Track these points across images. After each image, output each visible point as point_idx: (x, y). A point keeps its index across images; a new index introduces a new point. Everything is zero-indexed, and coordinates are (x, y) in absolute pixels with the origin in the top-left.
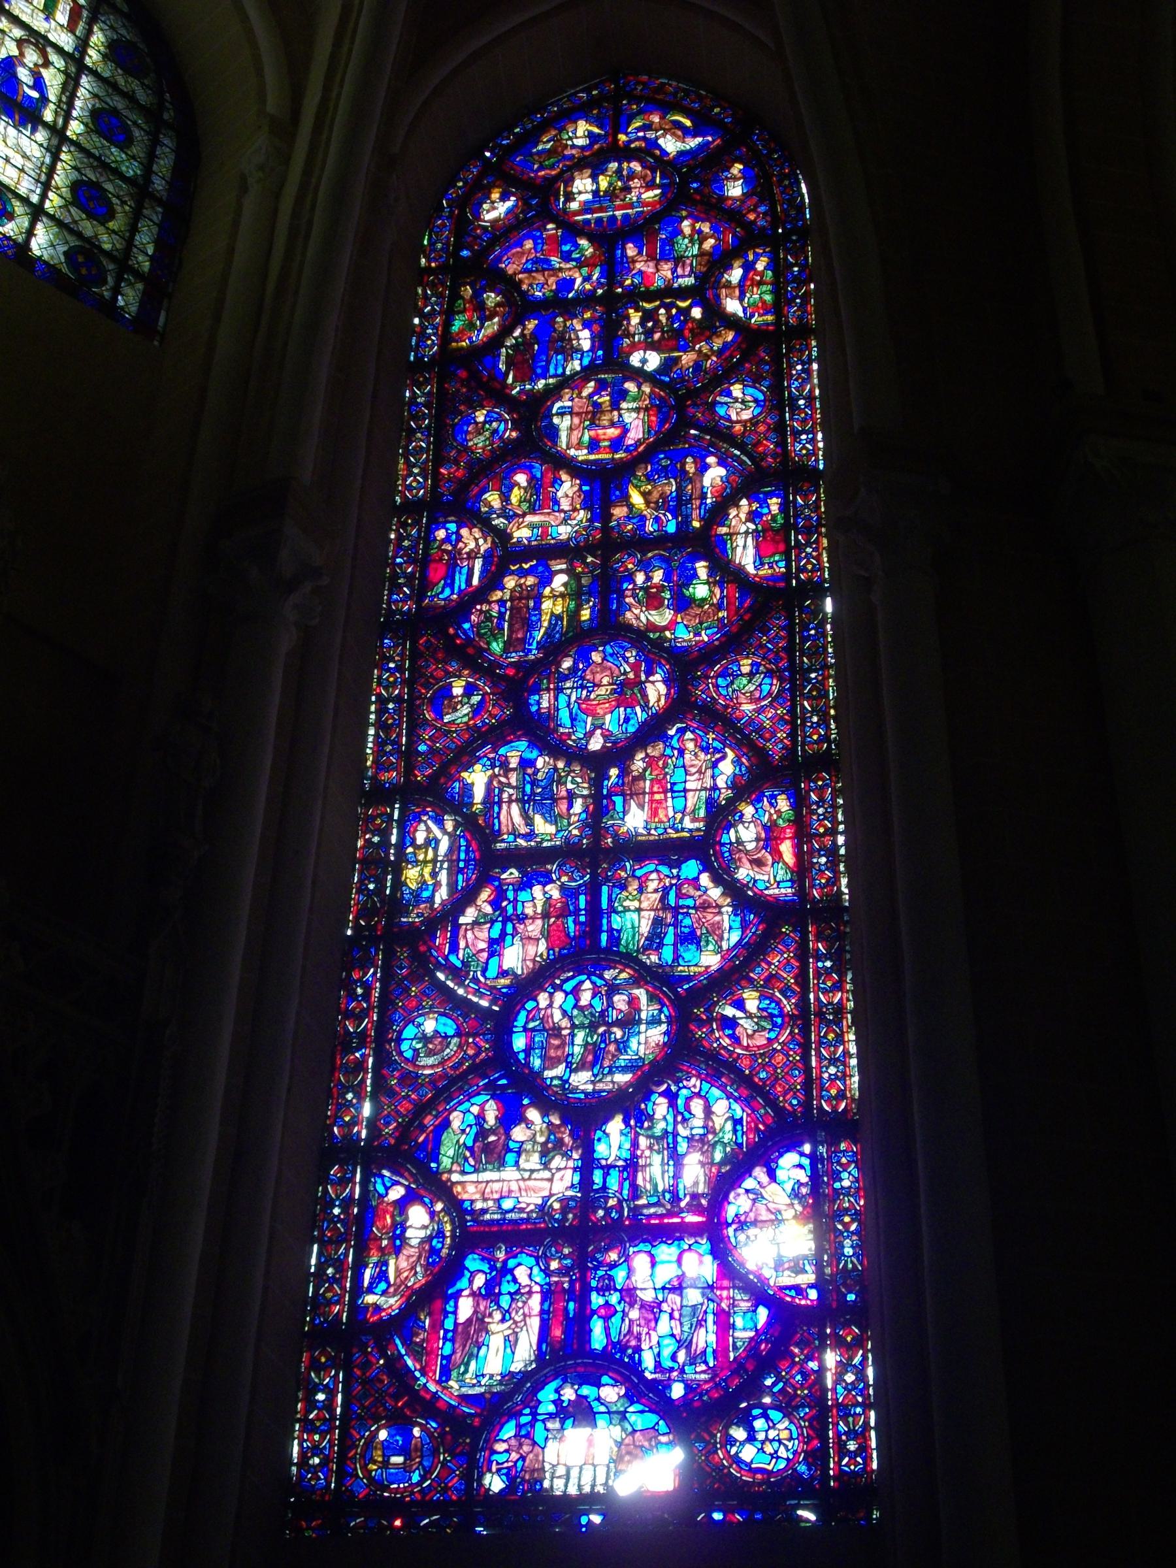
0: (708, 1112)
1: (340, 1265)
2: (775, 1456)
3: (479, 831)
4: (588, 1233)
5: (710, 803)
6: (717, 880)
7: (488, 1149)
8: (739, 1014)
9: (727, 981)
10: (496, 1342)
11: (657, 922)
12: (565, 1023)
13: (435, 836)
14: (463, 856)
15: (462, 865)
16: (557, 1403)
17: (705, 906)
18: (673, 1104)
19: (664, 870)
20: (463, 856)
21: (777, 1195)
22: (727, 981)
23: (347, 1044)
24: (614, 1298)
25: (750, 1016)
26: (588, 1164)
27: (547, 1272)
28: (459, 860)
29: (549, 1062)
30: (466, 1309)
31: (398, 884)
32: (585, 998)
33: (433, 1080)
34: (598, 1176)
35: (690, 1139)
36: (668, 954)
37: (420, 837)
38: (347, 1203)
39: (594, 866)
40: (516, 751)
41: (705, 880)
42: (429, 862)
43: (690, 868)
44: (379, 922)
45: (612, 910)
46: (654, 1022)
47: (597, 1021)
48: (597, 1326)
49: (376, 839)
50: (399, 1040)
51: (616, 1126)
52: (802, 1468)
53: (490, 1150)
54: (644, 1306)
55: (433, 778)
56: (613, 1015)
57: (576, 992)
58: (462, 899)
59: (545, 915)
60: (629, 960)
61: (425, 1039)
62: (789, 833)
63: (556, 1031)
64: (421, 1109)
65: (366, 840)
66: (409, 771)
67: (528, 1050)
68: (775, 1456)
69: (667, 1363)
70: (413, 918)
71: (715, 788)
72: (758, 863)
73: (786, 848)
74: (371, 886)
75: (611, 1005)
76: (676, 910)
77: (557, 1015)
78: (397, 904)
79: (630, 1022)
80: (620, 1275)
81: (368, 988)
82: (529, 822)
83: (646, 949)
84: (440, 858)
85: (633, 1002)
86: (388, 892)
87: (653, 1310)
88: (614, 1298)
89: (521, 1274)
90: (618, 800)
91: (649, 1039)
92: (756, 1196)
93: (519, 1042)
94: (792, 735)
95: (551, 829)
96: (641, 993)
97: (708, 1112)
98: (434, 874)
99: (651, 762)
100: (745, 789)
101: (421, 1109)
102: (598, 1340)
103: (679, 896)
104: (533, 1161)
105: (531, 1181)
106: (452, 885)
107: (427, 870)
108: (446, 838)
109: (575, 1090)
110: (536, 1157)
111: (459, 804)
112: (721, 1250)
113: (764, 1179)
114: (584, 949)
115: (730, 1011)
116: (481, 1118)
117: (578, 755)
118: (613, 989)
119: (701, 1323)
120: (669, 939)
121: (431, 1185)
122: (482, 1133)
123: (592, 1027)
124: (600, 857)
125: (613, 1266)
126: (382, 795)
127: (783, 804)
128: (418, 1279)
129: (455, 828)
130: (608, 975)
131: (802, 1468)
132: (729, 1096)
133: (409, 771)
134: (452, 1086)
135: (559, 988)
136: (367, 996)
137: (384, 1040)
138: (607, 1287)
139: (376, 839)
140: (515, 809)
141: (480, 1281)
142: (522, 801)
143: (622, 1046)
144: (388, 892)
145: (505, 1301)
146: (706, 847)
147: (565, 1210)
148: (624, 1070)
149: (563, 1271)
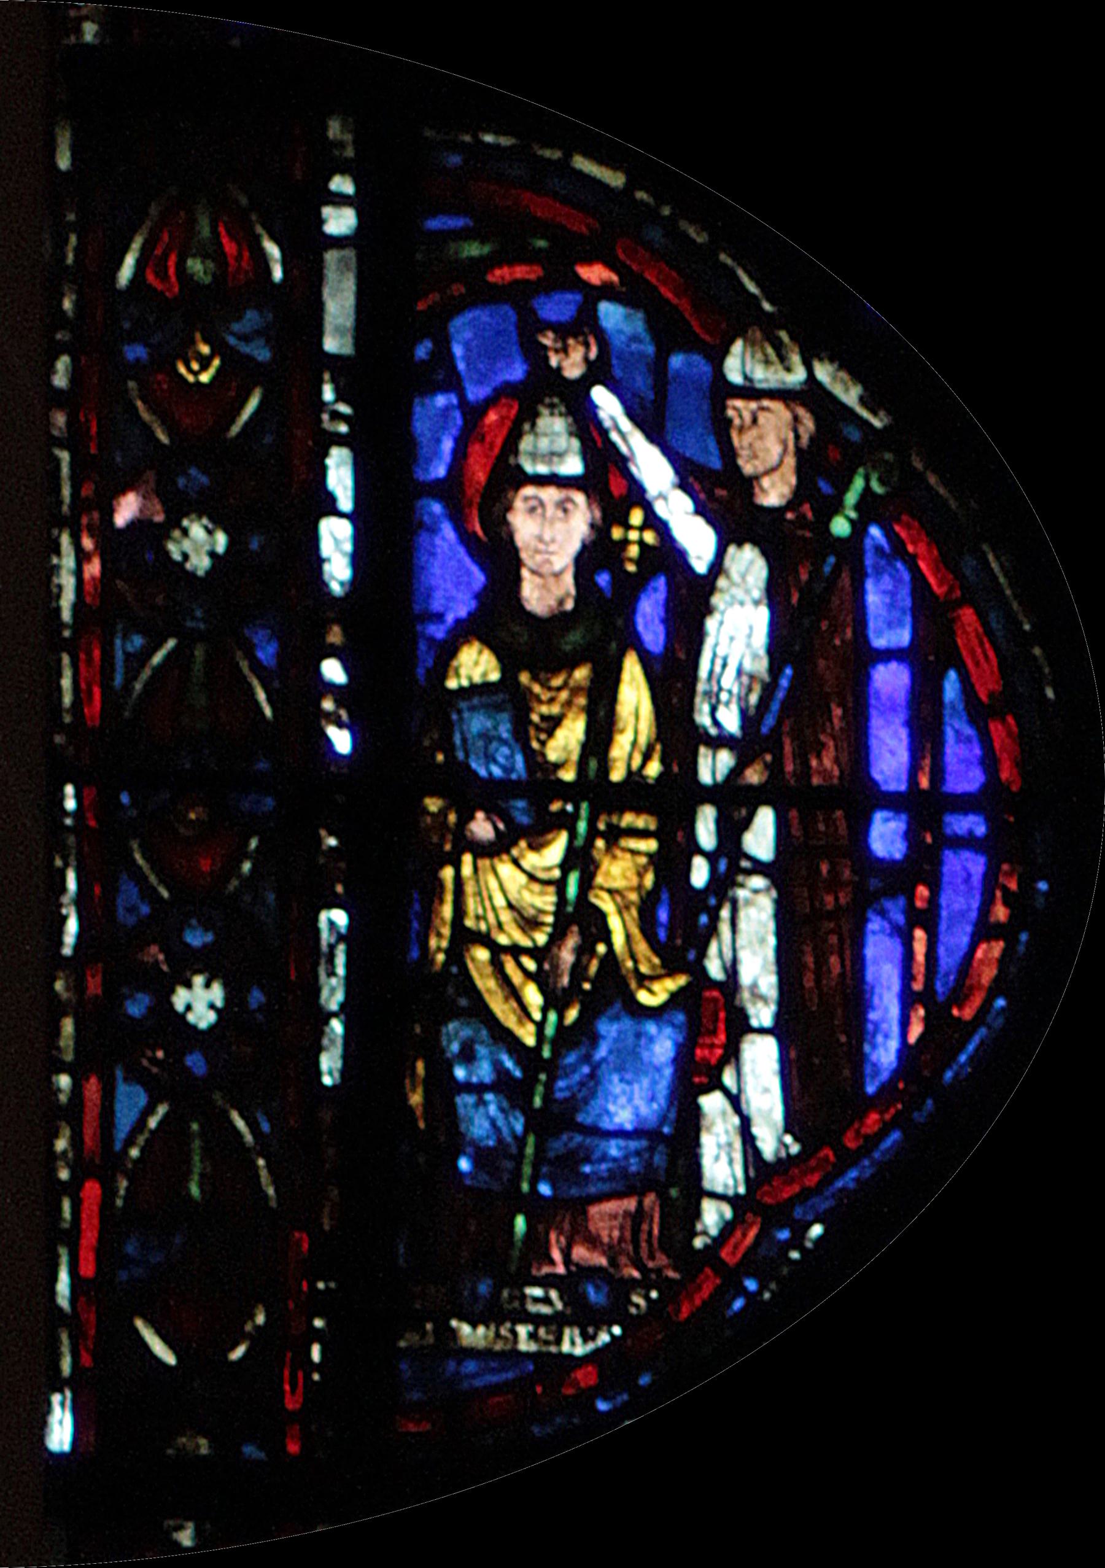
14: (890, 757)
15: (886, 836)
20: (890, 757)
28: (861, 796)
42: (634, 793)
44: (280, 1345)
49: (199, 544)
65: (111, 541)
74: (200, 1002)
84: (713, 766)
86: (330, 1065)
107: (620, 872)
108: (748, 566)
129: (820, 465)
139: (199, 544)
144: (330, 1065)
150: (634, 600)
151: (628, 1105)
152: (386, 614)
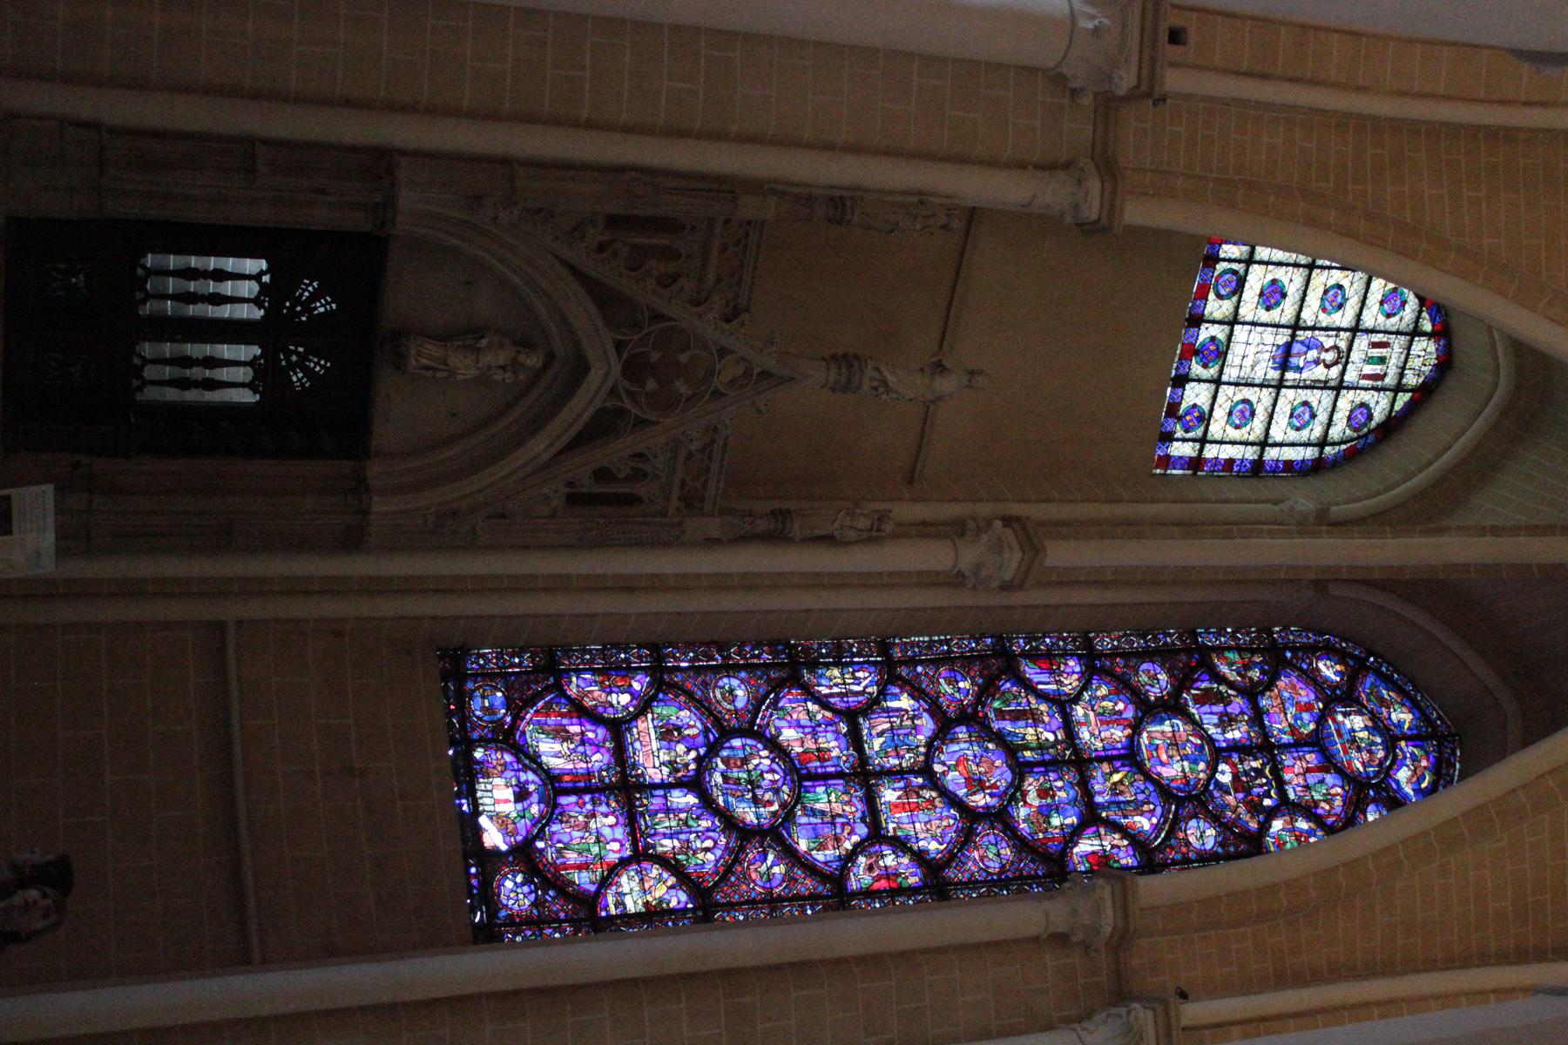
0: (707, 850)
1: (592, 661)
2: (509, 898)
3: (871, 706)
4: (626, 789)
5: (907, 837)
6: (856, 846)
7: (669, 732)
8: (769, 863)
9: (789, 854)
10: (557, 747)
11: (823, 813)
12: (751, 767)
13: (864, 681)
16: (527, 782)
17: (837, 839)
18: (708, 830)
19: (858, 815)
21: (660, 891)
22: (789, 854)
23: (722, 647)
24: (589, 807)
25: (768, 869)
26: (666, 786)
27: (601, 770)
29: (726, 761)
30: (575, 729)
31: (827, 666)
32: (768, 776)
33: (708, 699)
34: (661, 792)
35: (688, 841)
36: (804, 820)
37: (860, 674)
38: (626, 660)
39: (855, 774)
40: (927, 724)
41: (855, 839)
43: (862, 830)
45: (827, 786)
46: (758, 816)
47: (753, 784)
48: (573, 799)
50: (728, 676)
51: (691, 799)
52: (503, 913)
53: (668, 733)
54: (587, 823)
55: (900, 677)
56: (759, 792)
57: (772, 771)
58: (823, 702)
59: (818, 750)
60: (798, 800)
61: (731, 691)
62: (894, 885)
63: (745, 761)
64: (690, 695)
66: (901, 663)
67: (732, 748)
68: (509, 898)
69: (556, 837)
70: (806, 676)
71: (918, 839)
72: (870, 868)
73: (883, 884)
75: (766, 791)
76: (833, 824)
77: (755, 762)
78: (813, 665)
79: (756, 801)
80: (603, 809)
81: (758, 657)
82: (880, 735)
83: (804, 808)
85: (770, 803)
87: (586, 827)
88: (589, 807)
89: (598, 756)
90: (902, 784)
91: (747, 813)
92: (660, 879)
93: (737, 742)
94: (960, 883)
95: (877, 748)
96: (776, 807)
97: (707, 850)
98: (836, 685)
99: (931, 801)
100: (920, 857)
101: (690, 695)
102: (564, 800)
103: (843, 825)
104: (664, 757)
105: (652, 757)
106: (832, 695)
109: (711, 776)
110: (667, 758)
111: (883, 694)
112: (624, 863)
113: (669, 883)
114: (802, 774)
115: (771, 857)
116: (690, 727)
117: (929, 757)
118: (777, 791)
119: (580, 854)
120: (813, 820)
121: (644, 706)
122: (679, 728)
123: (750, 782)
124: (864, 776)
125: (608, 805)
126: (884, 648)
127: (913, 880)
128: (588, 703)
130: (785, 788)
131: (503, 913)
132: (717, 861)
133: (901, 663)
134: (704, 707)
135: (773, 761)
136: (754, 656)
137: (729, 669)
138: (593, 801)
140: (887, 726)
141: (591, 735)
142: (892, 728)
143: (741, 798)
145: (581, 749)
146: (877, 836)
147: (637, 776)
148: (726, 802)
149: (601, 779)
150: (858, 681)
151: (823, 682)
152: (852, 664)
